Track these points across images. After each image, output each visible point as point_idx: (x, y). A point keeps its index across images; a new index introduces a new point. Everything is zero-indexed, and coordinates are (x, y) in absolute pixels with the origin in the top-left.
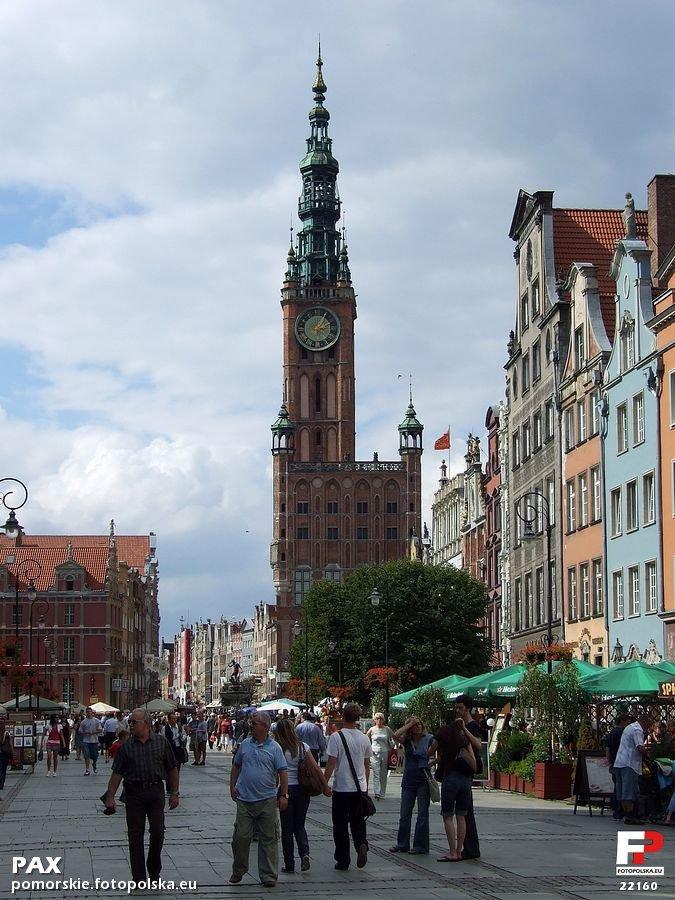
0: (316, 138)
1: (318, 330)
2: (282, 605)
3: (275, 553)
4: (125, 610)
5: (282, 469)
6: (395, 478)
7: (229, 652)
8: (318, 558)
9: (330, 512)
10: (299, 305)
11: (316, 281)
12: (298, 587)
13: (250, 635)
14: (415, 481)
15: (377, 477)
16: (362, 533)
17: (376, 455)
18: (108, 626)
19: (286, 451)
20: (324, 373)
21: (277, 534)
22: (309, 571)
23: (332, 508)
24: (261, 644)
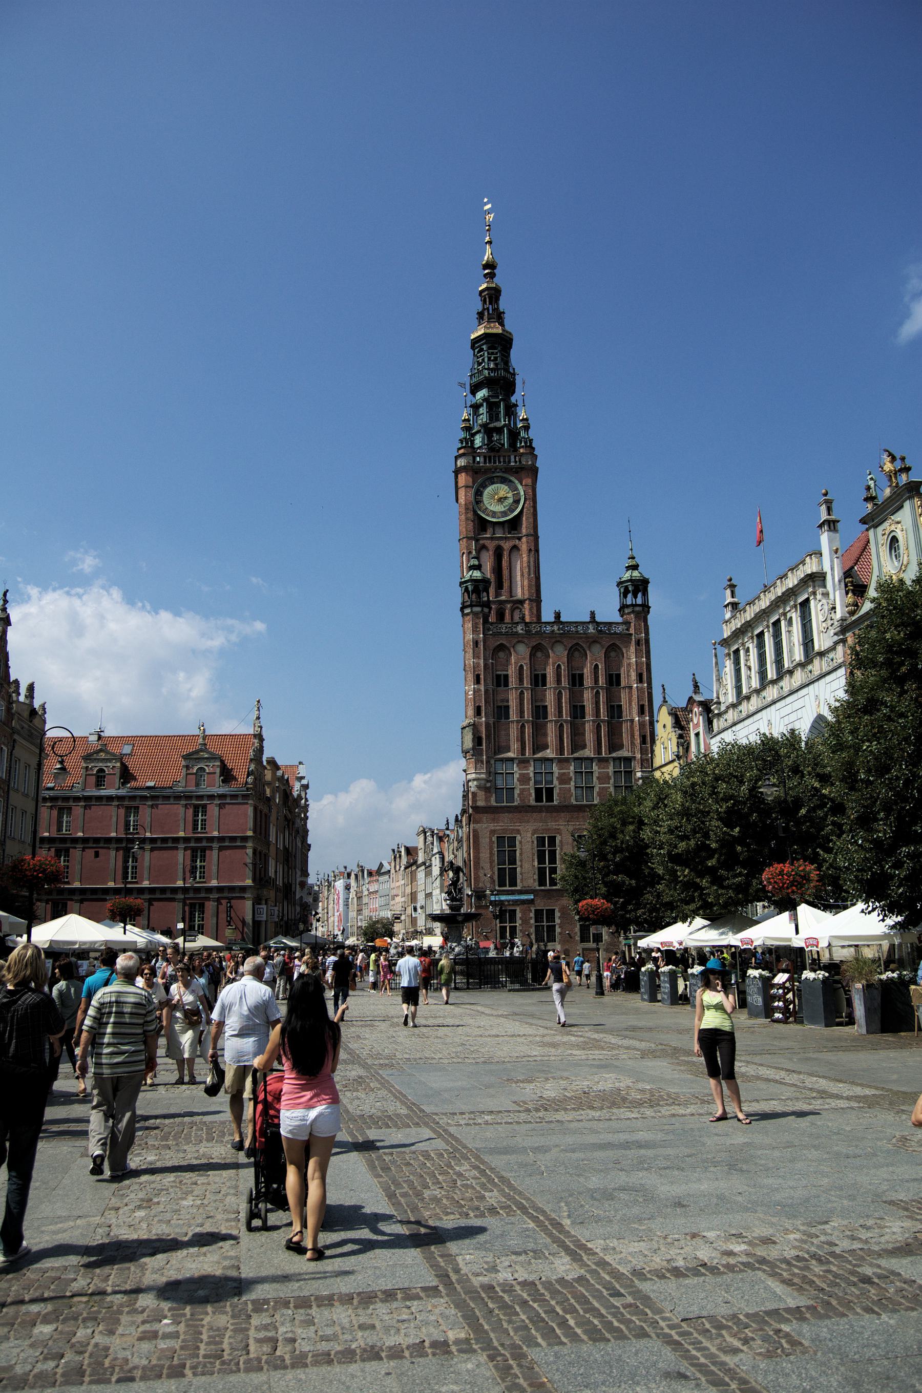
0: (488, 309)
1: (497, 500)
4: (273, 818)
5: (475, 630)
7: (366, 893)
9: (537, 685)
10: (476, 473)
11: (493, 450)
13: (387, 877)
14: (644, 646)
15: (595, 642)
17: (593, 614)
18: (250, 833)
19: (478, 609)
20: (507, 546)
21: (471, 712)
24: (398, 884)
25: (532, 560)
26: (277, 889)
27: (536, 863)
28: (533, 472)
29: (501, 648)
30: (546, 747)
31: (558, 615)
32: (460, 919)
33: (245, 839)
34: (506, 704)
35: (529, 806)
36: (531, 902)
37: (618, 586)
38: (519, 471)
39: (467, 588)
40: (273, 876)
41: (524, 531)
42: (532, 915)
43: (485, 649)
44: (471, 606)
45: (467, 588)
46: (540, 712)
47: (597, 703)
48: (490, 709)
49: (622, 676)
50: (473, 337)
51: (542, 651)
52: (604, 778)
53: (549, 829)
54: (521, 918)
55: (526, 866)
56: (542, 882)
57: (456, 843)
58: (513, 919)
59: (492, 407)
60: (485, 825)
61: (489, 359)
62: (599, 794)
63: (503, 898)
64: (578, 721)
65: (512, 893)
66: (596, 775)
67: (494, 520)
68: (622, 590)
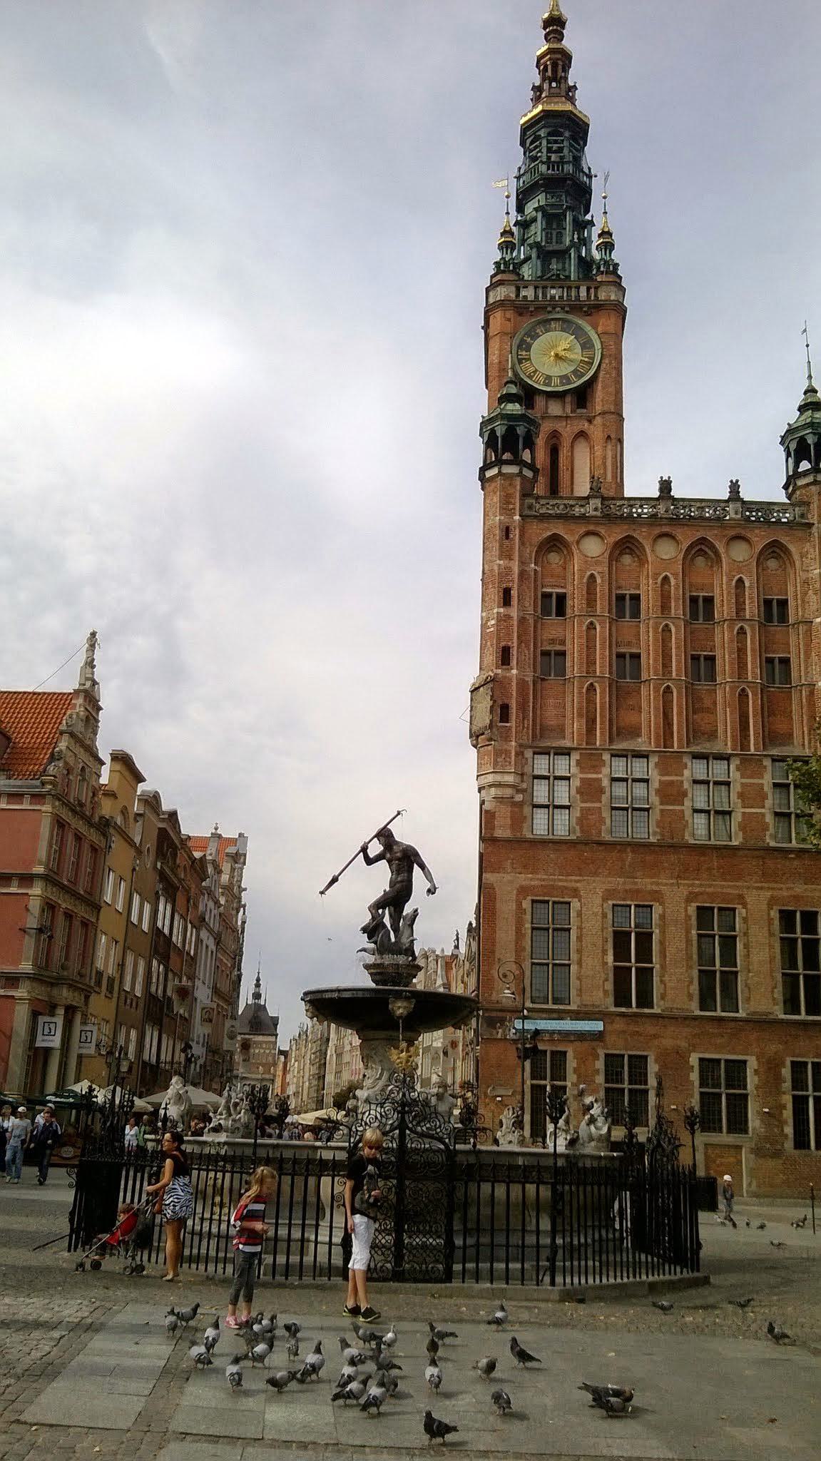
2: (499, 833)
3: (486, 703)
5: (506, 508)
6: (784, 540)
7: (348, 1048)
8: (591, 722)
9: (621, 614)
10: (521, 315)
12: (541, 793)
15: (738, 537)
16: (702, 666)
17: (735, 487)
18: (40, 869)
19: (513, 469)
20: (567, 431)
21: (491, 658)
22: (566, 752)
23: (626, 605)
25: (609, 454)
26: (127, 997)
27: (610, 958)
28: (620, 311)
29: (554, 543)
30: (635, 732)
31: (666, 486)
32: (400, 1008)
33: (27, 879)
34: (558, 648)
35: (600, 843)
36: (599, 1036)
37: (782, 443)
38: (593, 309)
39: (493, 431)
40: (111, 970)
41: (599, 408)
42: (600, 1064)
43: (522, 543)
44: (500, 462)
45: (493, 431)
46: (627, 663)
47: (741, 651)
48: (529, 653)
49: (791, 604)
50: (522, 122)
51: (632, 552)
52: (752, 796)
53: (638, 891)
54: (575, 1070)
55: (591, 962)
56: (621, 997)
57: (467, 964)
58: (559, 1072)
59: (552, 219)
60: (508, 877)
61: (549, 150)
62: (743, 827)
63: (543, 1025)
64: (703, 686)
65: (560, 1015)
66: (736, 788)
67: (549, 389)
68: (793, 446)
